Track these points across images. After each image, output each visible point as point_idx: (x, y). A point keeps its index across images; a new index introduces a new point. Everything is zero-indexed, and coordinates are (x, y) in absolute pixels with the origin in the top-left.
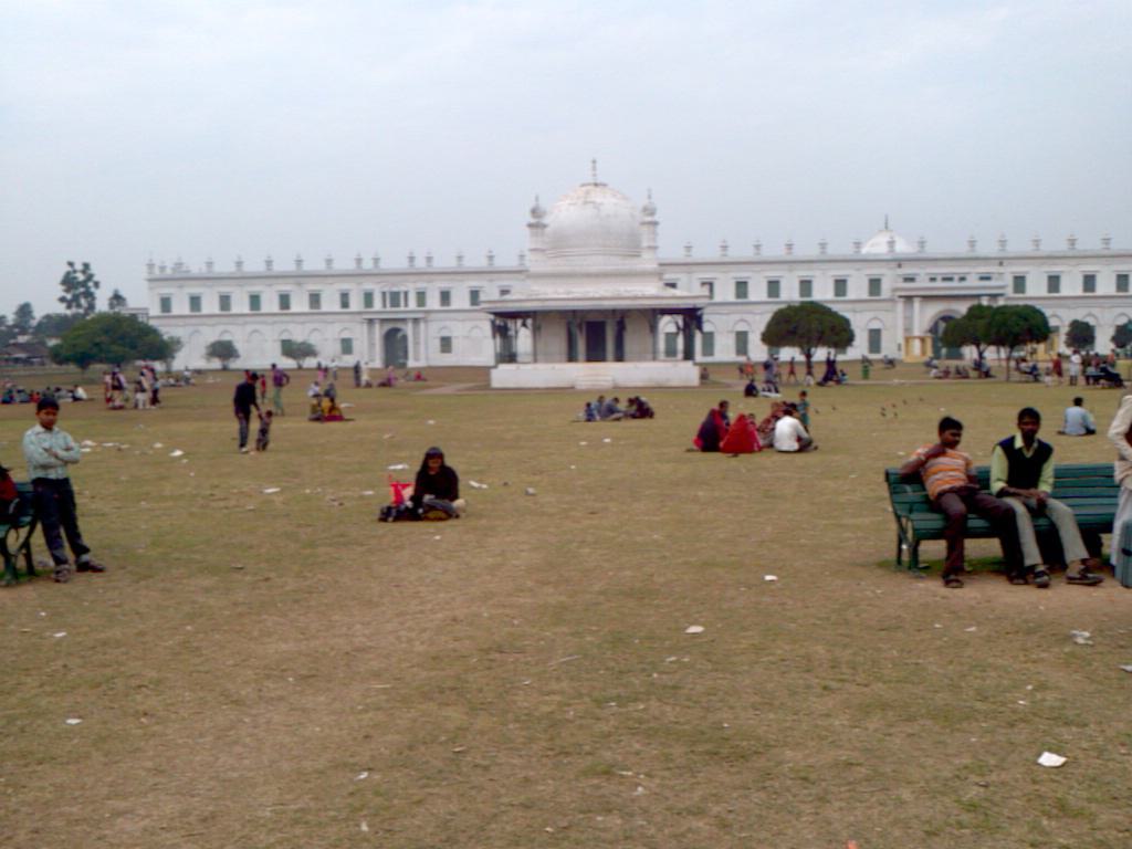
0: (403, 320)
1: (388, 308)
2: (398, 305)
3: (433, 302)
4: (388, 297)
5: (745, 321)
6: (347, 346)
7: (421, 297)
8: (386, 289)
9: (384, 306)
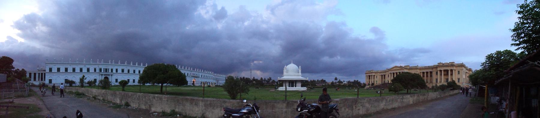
0: (109, 75)
1: (105, 72)
2: (107, 72)
3: (114, 71)
5: (75, 77)
8: (105, 68)
9: (104, 72)
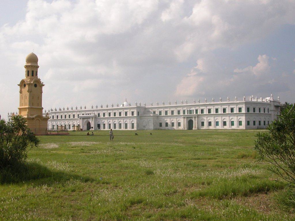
1: (189, 114)
6: (179, 124)
7: (197, 111)
8: (188, 109)
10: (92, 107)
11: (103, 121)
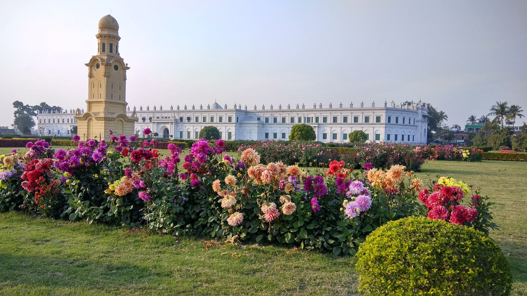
1: (306, 123)
3: (321, 121)
4: (306, 118)
7: (317, 119)
10: (172, 108)
11: (187, 128)
